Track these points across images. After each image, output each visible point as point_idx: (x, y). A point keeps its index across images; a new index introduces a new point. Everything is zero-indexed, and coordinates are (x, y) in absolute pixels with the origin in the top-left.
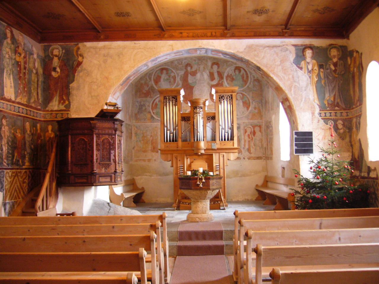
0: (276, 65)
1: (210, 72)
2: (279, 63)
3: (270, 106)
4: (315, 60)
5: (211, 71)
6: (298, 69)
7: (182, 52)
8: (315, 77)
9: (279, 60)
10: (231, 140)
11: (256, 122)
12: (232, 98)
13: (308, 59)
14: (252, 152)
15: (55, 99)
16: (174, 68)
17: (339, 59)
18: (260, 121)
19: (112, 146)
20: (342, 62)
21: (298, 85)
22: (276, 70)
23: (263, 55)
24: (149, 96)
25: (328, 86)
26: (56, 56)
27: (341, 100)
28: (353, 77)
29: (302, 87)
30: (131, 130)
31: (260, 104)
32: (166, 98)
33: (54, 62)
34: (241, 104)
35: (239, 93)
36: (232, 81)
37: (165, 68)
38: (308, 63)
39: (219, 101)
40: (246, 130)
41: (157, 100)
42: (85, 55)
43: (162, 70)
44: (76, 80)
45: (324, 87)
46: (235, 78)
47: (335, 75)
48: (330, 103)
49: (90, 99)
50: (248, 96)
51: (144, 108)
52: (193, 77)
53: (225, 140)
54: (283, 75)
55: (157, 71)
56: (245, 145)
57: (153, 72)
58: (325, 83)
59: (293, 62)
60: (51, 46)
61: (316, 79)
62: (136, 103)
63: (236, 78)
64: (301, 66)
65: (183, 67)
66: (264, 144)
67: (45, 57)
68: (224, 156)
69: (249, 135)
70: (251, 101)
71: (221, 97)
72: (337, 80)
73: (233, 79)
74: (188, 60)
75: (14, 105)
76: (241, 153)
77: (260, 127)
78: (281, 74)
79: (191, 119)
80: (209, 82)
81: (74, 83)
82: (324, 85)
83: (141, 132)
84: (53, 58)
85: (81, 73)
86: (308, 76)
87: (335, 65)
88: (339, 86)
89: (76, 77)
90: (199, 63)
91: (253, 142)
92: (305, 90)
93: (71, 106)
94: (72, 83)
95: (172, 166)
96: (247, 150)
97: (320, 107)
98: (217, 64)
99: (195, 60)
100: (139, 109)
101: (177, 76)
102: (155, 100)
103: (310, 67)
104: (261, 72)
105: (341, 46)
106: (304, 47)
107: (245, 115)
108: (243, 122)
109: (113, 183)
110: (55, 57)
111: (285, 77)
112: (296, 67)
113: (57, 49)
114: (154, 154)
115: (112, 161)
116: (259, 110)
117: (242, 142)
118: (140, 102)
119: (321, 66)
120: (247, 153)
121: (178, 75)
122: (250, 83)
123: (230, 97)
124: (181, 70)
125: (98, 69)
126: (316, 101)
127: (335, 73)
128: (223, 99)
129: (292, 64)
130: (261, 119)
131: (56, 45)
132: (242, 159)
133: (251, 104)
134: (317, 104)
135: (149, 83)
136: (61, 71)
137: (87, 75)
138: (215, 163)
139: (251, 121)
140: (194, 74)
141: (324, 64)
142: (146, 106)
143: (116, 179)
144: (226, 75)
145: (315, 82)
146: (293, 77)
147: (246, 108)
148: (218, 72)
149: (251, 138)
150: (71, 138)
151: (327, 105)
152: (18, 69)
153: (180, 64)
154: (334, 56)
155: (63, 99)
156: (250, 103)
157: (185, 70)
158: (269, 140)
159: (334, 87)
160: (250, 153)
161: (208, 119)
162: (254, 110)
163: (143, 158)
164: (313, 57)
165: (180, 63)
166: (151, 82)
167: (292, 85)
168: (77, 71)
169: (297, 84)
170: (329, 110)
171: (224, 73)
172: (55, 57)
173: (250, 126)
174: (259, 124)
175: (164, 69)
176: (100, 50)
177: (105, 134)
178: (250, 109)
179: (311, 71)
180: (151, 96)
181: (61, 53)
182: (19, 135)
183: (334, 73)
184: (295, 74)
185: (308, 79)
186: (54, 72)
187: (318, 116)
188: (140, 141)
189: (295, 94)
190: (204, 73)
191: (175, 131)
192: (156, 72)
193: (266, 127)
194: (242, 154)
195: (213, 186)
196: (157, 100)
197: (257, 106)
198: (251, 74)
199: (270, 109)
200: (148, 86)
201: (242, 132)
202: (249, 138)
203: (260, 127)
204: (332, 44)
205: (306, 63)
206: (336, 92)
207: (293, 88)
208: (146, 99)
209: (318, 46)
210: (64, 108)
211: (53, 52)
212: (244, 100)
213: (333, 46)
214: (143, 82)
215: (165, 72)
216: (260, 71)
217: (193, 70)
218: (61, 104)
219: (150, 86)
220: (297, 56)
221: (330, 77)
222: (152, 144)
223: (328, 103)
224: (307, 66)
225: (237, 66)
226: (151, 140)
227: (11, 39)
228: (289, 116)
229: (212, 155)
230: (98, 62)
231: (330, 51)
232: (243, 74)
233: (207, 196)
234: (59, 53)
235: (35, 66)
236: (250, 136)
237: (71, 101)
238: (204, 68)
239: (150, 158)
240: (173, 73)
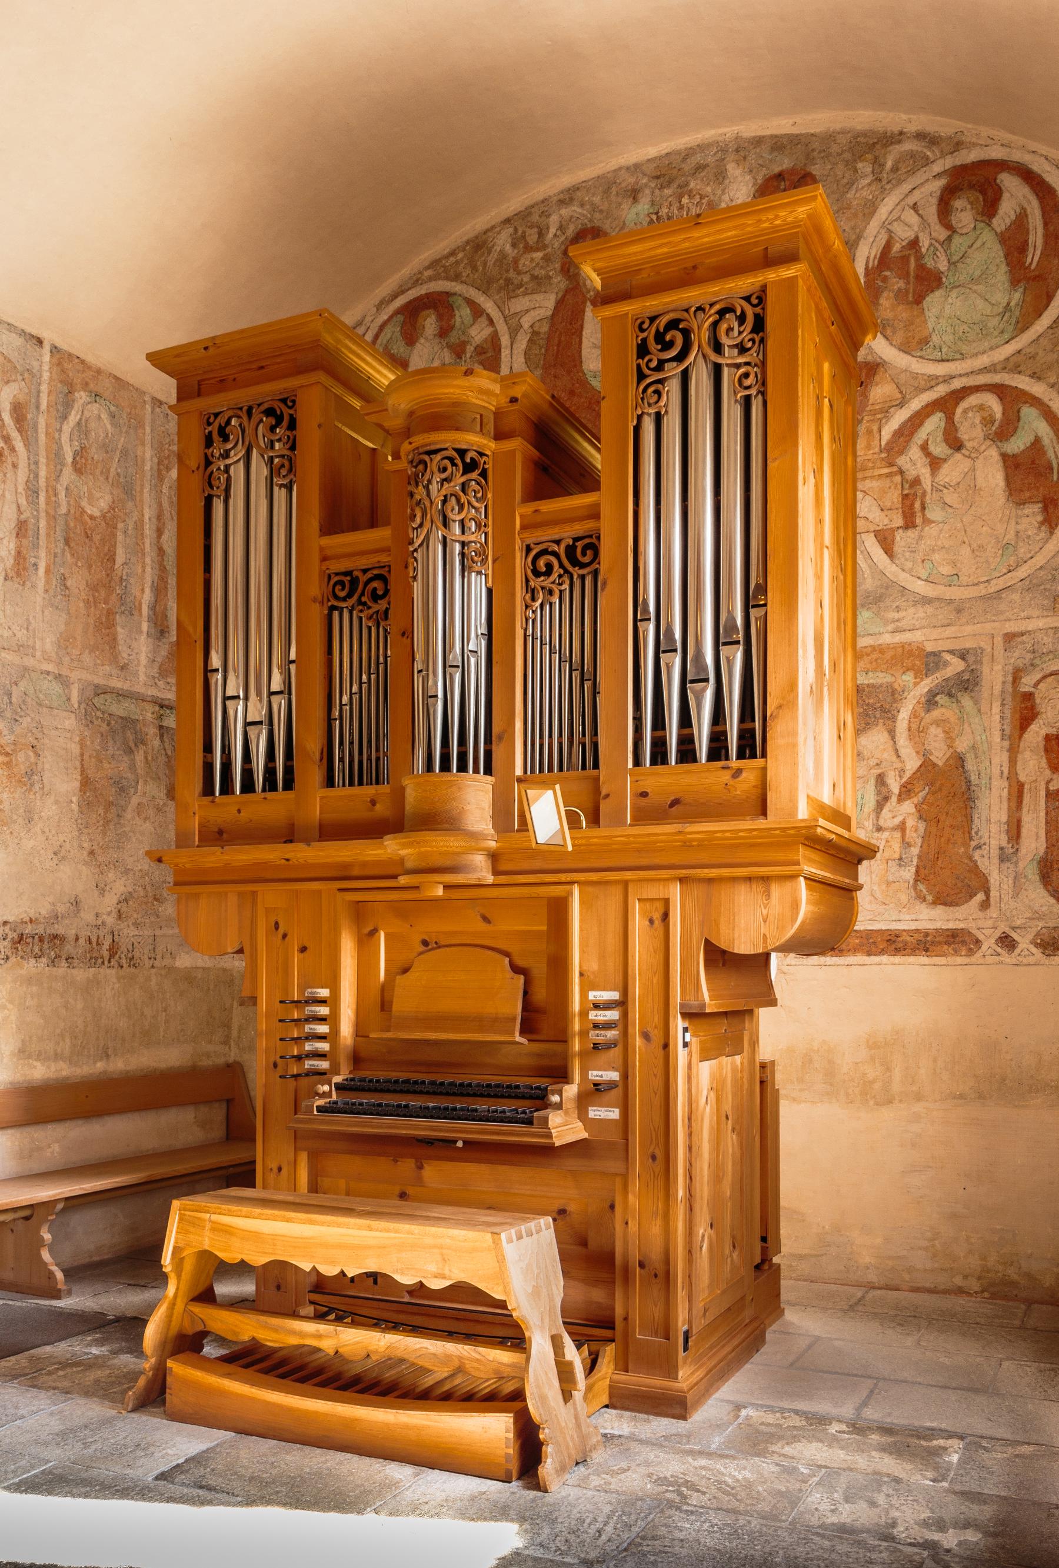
12: (759, 325)
37: (428, 295)
40: (1029, 697)
56: (1015, 831)
71: (659, 337)
74: (582, 205)
76: (980, 897)
96: (1033, 874)
101: (505, 340)
107: (1022, 572)
108: (1010, 638)
128: (673, 353)
132: (989, 944)
153: (528, 249)
165: (532, 237)
194: (985, 905)
232: (1022, 218)
240: (483, 319)
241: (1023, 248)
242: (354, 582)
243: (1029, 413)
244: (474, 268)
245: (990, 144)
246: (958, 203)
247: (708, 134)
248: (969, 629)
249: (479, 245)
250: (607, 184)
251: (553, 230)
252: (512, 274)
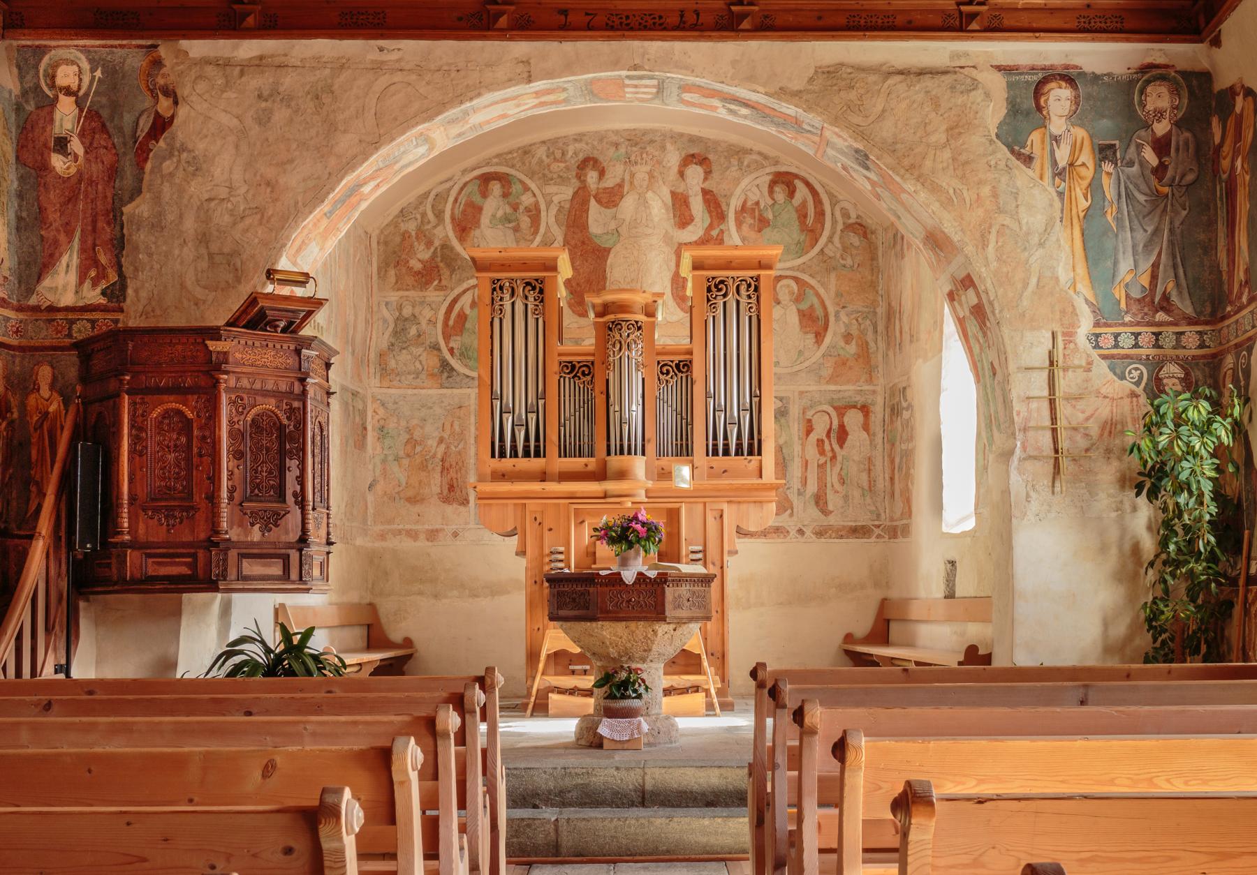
0: (928, 145)
1: (674, 194)
2: (939, 137)
3: (906, 328)
4: (1082, 126)
5: (680, 190)
6: (1014, 162)
7: (565, 90)
8: (1079, 193)
9: (944, 127)
10: (751, 453)
11: (847, 391)
12: (756, 289)
13: (1057, 125)
14: (830, 507)
15: (65, 260)
16: (532, 175)
17: (1178, 124)
18: (866, 387)
19: (292, 440)
20: (1187, 134)
21: (1014, 226)
22: (928, 163)
23: (879, 108)
24: (436, 283)
25: (1132, 230)
26: (68, 91)
27: (1178, 285)
28: (1231, 193)
29: (1028, 234)
30: (363, 414)
31: (868, 322)
32: (501, 288)
33: (57, 116)
34: (794, 319)
35: (786, 277)
36: (760, 231)
38: (1056, 139)
39: (708, 300)
40: (809, 421)
41: (466, 300)
42: (184, 91)
43: (486, 179)
44: (149, 190)
45: (1117, 236)
46: (771, 217)
47: (1160, 188)
48: (1136, 294)
49: (204, 264)
50: (822, 291)
51: (413, 331)
52: (609, 211)
53: (726, 452)
54: (956, 183)
55: (465, 184)
56: (804, 482)
57: (449, 190)
58: (1118, 220)
59: (997, 135)
60: (49, 48)
61: (1084, 204)
62: (385, 311)
63: (775, 217)
64: (1026, 151)
65: (567, 168)
66: (881, 478)
67: (24, 93)
68: (721, 516)
69: (820, 442)
70: (831, 309)
72: (1166, 206)
73: (763, 223)
77: (865, 409)
78: (948, 182)
79: (597, 370)
80: (670, 230)
81: (138, 200)
82: (1114, 225)
83: (403, 423)
84: (57, 98)
85: (168, 162)
86: (1051, 190)
87: (1162, 146)
88: (1171, 231)
89: (147, 177)
90: (633, 158)
91: (837, 469)
92: (1041, 245)
93: (130, 291)
94: (132, 199)
95: (521, 553)
97: (1096, 310)
98: (703, 161)
99: (617, 145)
100: (395, 333)
101: (543, 207)
102: (455, 301)
103: (1063, 155)
104: (872, 176)
105: (1185, 74)
106: (1040, 76)
108: (801, 393)
109: (293, 582)
110: (61, 97)
111: (965, 192)
112: (1009, 155)
113: (73, 63)
114: (449, 509)
115: (290, 499)
116: (864, 347)
117: (795, 470)
118: (400, 308)
119: (1105, 152)
120: (814, 512)
121: (549, 204)
122: (830, 239)
123: (749, 286)
124: (563, 180)
125: (237, 147)
126: (1079, 287)
127: (1160, 180)
129: (991, 141)
130: (870, 380)
133: (832, 319)
134: (1086, 300)
135: (435, 231)
136: (86, 152)
137: (191, 169)
138: (689, 543)
139: (833, 387)
140: (611, 198)
141: (1117, 142)
142: (424, 323)
143: (306, 567)
144: (735, 203)
145: (1082, 215)
146: (995, 195)
147: (810, 338)
148: (705, 192)
149: (830, 454)
150: (133, 404)
151: (1123, 305)
154: (1159, 114)
155: (96, 263)
156: (826, 316)
157: (575, 183)
158: (897, 460)
159: (1157, 231)
160: (825, 512)
161: (664, 370)
162: (842, 344)
163: (408, 527)
164: (1074, 117)
165: (558, 154)
166: (440, 228)
167: (990, 226)
168: (151, 155)
169: (1008, 221)
170: (1131, 324)
171: (728, 197)
172: (61, 97)
173: (830, 410)
174: (860, 400)
175: (494, 179)
176: (242, 74)
178: (828, 340)
179: (1064, 169)
180: (444, 283)
181: (86, 80)
183: (1154, 181)
184: (1004, 179)
185: (1052, 200)
186: (61, 157)
187: (1089, 346)
188: (397, 459)
189: (999, 259)
190: (650, 195)
191: (532, 417)
192: (462, 189)
193: (888, 410)
195: (679, 606)
196: (466, 300)
197: (855, 332)
198: (834, 201)
199: (906, 337)
200: (429, 243)
201: (796, 429)
202: (822, 452)
203: (865, 409)
204: (1152, 66)
205: (1048, 139)
206: (1160, 254)
207: (993, 238)
208: (421, 294)
209: (1098, 72)
210: (103, 301)
211: (53, 77)
212: (804, 306)
213: (1155, 72)
214: (411, 227)
215: (496, 188)
216: (867, 168)
217: (609, 182)
218: (87, 284)
219: (437, 243)
220: (1014, 110)
221: (1137, 194)
222: (444, 470)
223: (1127, 296)
224: (1052, 152)
225: (783, 169)
226: (439, 456)
228: (976, 349)
229: (678, 511)
231: (1142, 92)
232: (804, 204)
233: (655, 648)
234: (80, 80)
236: (827, 447)
237: (128, 270)
238: (651, 175)
239: (438, 527)
240: (529, 193)
241: (805, 216)
242: (573, 367)
243: (809, 292)
244: (524, 163)
245: (789, 165)
246: (777, 189)
247: (656, 125)
248: (783, 388)
249: (526, 151)
250: (601, 137)
251: (570, 153)
252: (546, 172)
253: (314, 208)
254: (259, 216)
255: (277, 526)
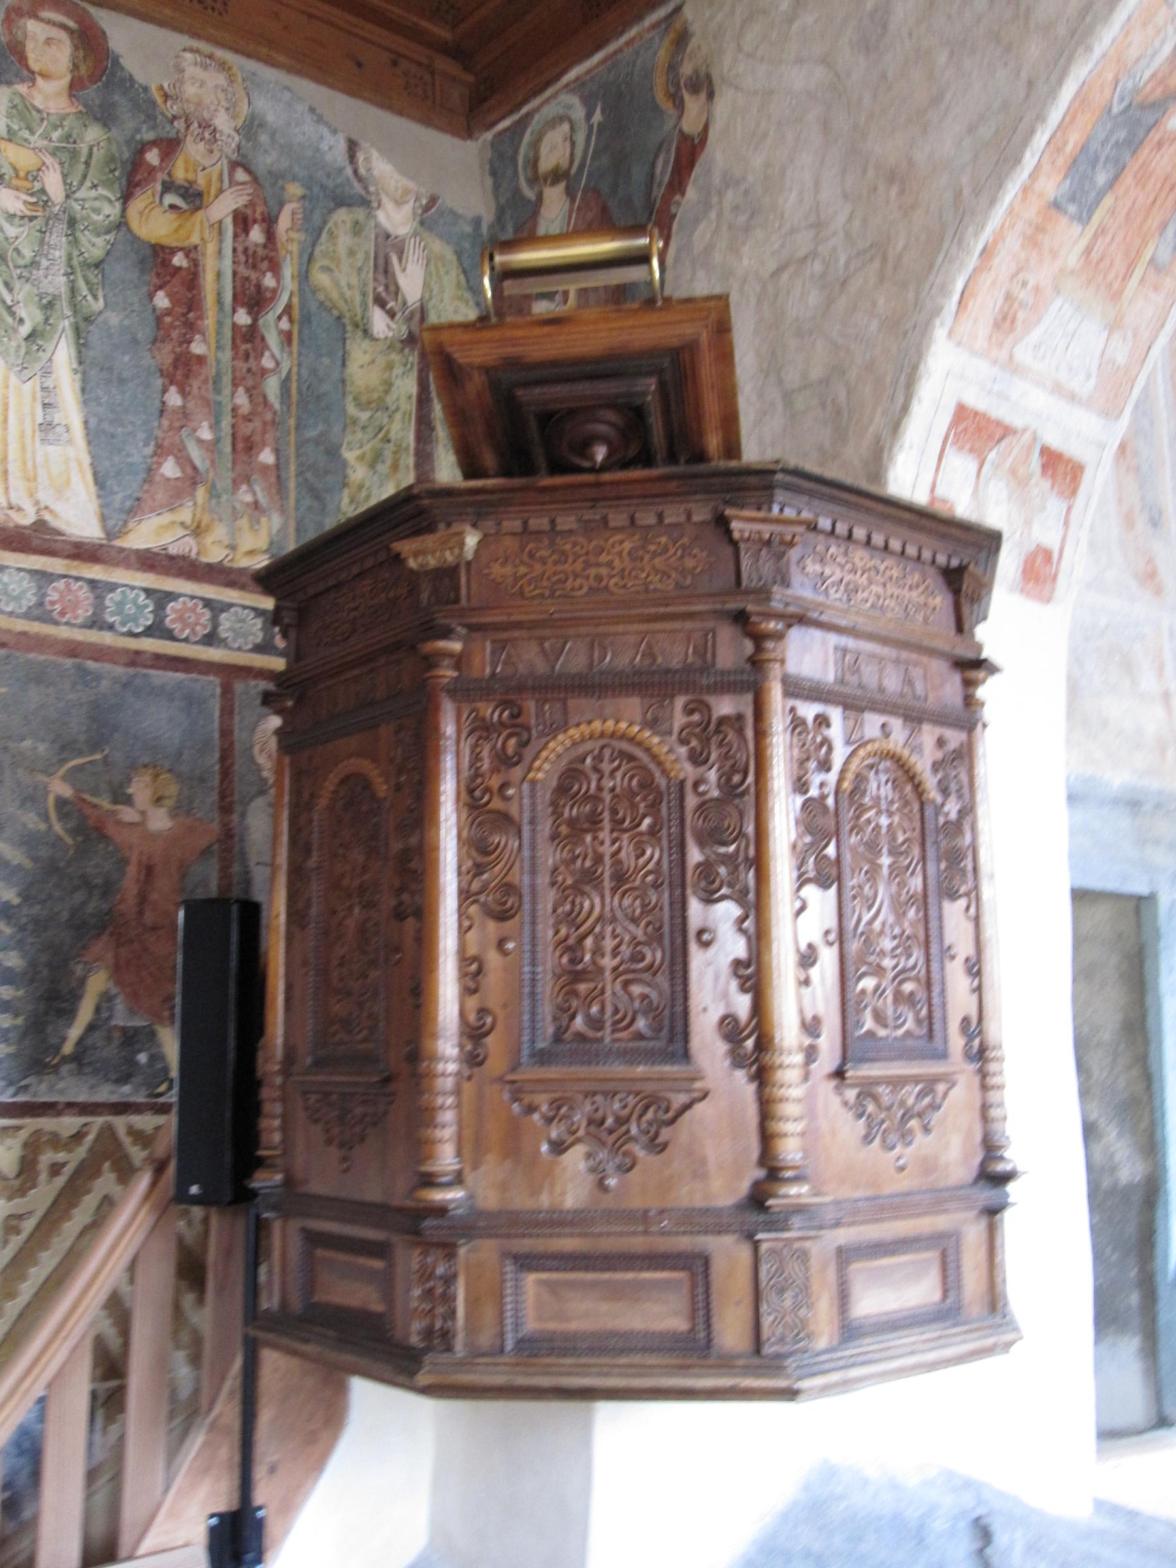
26: (556, 176)
60: (529, 116)
75: (96, 572)
113: (561, 119)
125: (826, 126)
131: (555, 96)
137: (742, 219)
152: (162, 301)
177: (596, 686)
182: (160, 821)
227: (75, 87)
230: (820, 73)
235: (395, 290)
253: (1000, 186)
254: (876, 264)
255: (657, 1147)
